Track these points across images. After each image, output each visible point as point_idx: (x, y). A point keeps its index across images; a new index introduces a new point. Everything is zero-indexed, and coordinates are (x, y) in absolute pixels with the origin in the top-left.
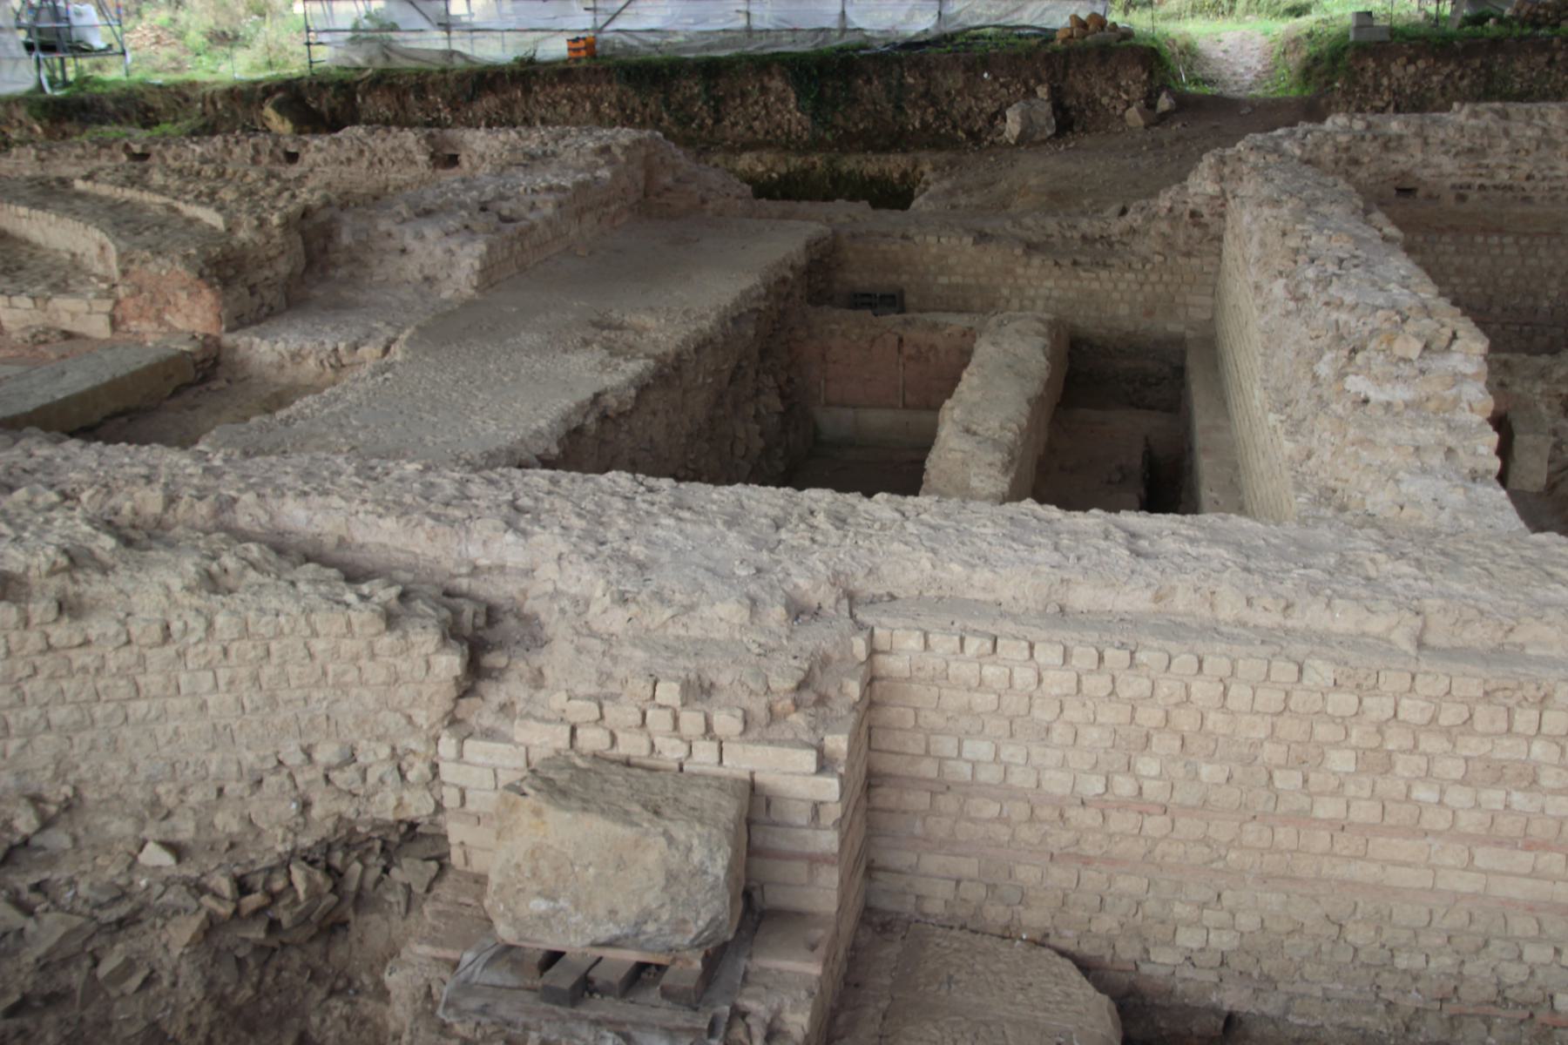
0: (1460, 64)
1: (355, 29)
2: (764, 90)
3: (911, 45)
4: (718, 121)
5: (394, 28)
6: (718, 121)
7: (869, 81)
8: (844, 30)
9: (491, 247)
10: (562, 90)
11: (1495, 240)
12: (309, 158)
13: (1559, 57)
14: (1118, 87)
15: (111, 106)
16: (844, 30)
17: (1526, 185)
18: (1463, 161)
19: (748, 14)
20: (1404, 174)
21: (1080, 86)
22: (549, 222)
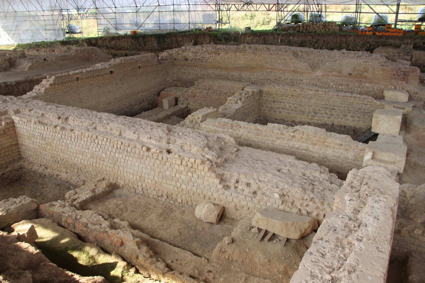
0: (259, 38)
1: (104, 29)
2: (151, 40)
3: (184, 32)
4: (145, 46)
5: (109, 29)
6: (145, 46)
7: (167, 39)
8: (174, 30)
9: (32, 64)
10: (123, 40)
11: (196, 68)
12: (55, 51)
13: (276, 37)
14: (206, 41)
15: (72, 42)
16: (174, 30)
17: (202, 59)
18: (194, 54)
19: (160, 27)
20: (185, 56)
21: (200, 41)
22: (53, 61)
